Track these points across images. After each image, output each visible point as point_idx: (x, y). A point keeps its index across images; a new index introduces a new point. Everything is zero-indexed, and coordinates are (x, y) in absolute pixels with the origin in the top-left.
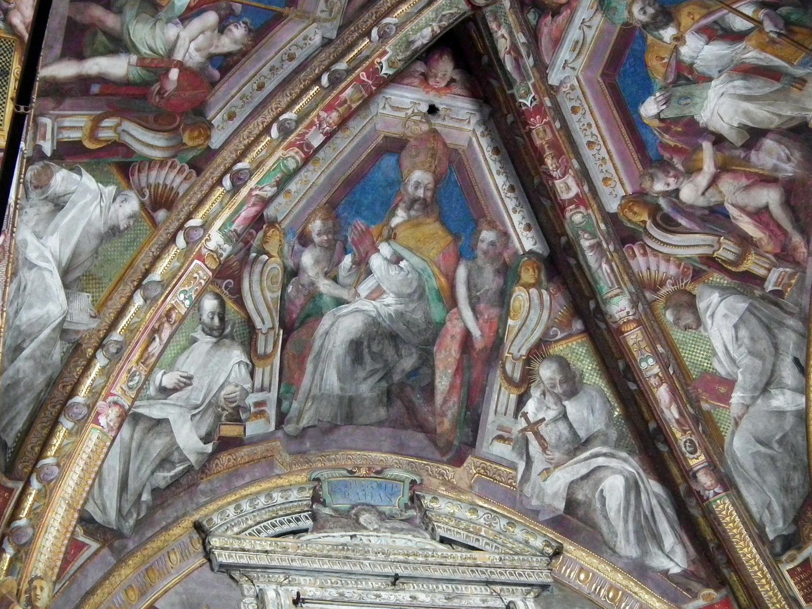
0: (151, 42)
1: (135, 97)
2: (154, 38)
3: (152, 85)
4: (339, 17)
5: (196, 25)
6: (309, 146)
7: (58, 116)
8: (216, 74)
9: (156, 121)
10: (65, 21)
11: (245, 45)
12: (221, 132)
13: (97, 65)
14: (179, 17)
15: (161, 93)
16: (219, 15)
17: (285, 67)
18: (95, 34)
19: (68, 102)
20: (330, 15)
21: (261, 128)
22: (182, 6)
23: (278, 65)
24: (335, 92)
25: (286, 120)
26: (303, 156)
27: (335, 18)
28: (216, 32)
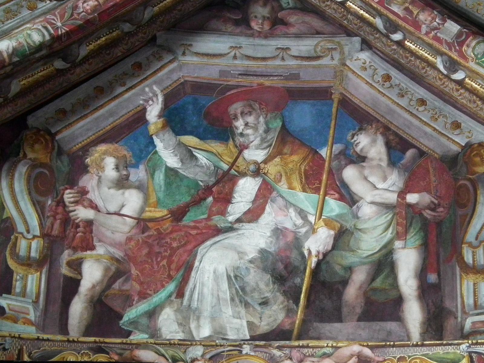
1: (439, 234)
2: (375, 228)
3: (425, 219)
4: (337, 39)
6: (459, 35)
7: (464, 312)
8: (410, 153)
9: (464, 206)
10: (362, 324)
11: (377, 129)
12: (475, 134)
13: (407, 281)
14: (351, 207)
15: (433, 207)
16: (346, 165)
17: (397, 82)
18: (375, 290)
19: (448, 304)
20: (335, 49)
21: (462, 91)
22: (339, 206)
23: (397, 90)
24: (400, 22)
25: (445, 67)
26: (471, 38)
27: (339, 43)
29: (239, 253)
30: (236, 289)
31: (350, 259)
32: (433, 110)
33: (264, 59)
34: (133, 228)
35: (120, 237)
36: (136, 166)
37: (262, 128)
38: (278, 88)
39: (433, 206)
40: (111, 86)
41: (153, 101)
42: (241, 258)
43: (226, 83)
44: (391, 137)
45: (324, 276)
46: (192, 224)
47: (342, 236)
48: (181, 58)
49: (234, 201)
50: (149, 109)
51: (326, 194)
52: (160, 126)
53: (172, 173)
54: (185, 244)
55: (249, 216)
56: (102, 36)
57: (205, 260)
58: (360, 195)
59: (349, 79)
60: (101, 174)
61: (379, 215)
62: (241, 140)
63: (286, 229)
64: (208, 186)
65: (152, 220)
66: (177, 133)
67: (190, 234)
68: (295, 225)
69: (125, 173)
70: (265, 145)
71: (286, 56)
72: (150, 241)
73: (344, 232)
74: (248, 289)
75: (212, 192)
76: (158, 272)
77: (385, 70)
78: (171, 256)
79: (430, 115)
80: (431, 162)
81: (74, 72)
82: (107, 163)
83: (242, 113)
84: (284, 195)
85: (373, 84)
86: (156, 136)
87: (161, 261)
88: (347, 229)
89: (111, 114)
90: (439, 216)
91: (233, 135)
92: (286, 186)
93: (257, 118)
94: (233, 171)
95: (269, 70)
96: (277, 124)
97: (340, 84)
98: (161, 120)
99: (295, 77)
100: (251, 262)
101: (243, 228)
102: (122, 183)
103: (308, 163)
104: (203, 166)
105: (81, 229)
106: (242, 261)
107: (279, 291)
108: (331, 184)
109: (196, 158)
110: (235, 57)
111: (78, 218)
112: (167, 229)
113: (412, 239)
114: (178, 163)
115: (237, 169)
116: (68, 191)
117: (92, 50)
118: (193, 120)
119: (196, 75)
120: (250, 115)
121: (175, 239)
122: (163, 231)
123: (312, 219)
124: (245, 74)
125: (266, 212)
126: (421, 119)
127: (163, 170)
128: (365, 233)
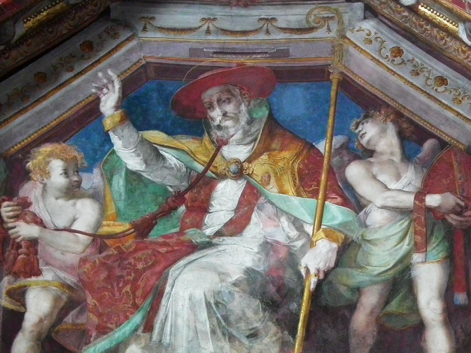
0: (394, 241)
2: (388, 238)
3: (450, 225)
5: (365, 188)
8: (428, 144)
11: (387, 116)
15: (459, 211)
16: (350, 161)
17: (410, 57)
20: (332, 18)
23: (410, 67)
27: (336, 10)
28: (372, 160)
29: (220, 274)
30: (218, 318)
31: (357, 277)
32: (456, 90)
33: (244, 33)
34: (87, 247)
35: (72, 259)
36: (89, 170)
37: (244, 119)
38: (263, 69)
39: (459, 210)
40: (56, 72)
41: (108, 88)
42: (222, 281)
43: (197, 64)
44: (405, 126)
45: (327, 299)
46: (161, 240)
47: (348, 250)
48: (141, 35)
49: (212, 209)
50: (103, 99)
51: (325, 198)
52: (117, 119)
53: (134, 177)
54: (153, 265)
55: (231, 228)
56: (42, 10)
57: (178, 283)
58: (368, 198)
59: (351, 55)
60: (46, 181)
61: (392, 222)
62: (219, 133)
63: (278, 242)
64: (179, 193)
65: (110, 236)
66: (140, 127)
67: (159, 252)
68: (289, 237)
69: (75, 178)
70: (249, 139)
71: (271, 29)
72: (109, 262)
73: (349, 245)
74: (232, 318)
75: (184, 199)
76: (121, 300)
77: (395, 42)
78: (136, 280)
79: (452, 96)
80: (455, 155)
81: (9, 56)
82: (52, 167)
83: (219, 101)
84: (274, 201)
85: (381, 60)
86: (113, 132)
87: (123, 287)
88: (353, 241)
89: (57, 106)
90: (467, 221)
91: (209, 128)
92: (275, 190)
93: (238, 106)
94: (209, 173)
95: (250, 47)
96: (263, 113)
97: (339, 61)
98: (119, 111)
99: (284, 54)
100: (235, 284)
101: (224, 242)
102: (73, 192)
103: (303, 160)
104: (172, 168)
105: (23, 250)
106: (224, 284)
107: (271, 319)
108: (331, 186)
109: (164, 158)
110: (208, 32)
111: (19, 236)
112: (130, 246)
113: (434, 251)
114: (141, 165)
115: (214, 170)
116: (5, 203)
117: (31, 28)
118: (159, 111)
119: (160, 55)
120: (229, 102)
121: (140, 260)
122: (125, 250)
123: (309, 229)
124: (221, 52)
125: (252, 222)
126: (441, 102)
127: (123, 173)
128: (375, 245)
